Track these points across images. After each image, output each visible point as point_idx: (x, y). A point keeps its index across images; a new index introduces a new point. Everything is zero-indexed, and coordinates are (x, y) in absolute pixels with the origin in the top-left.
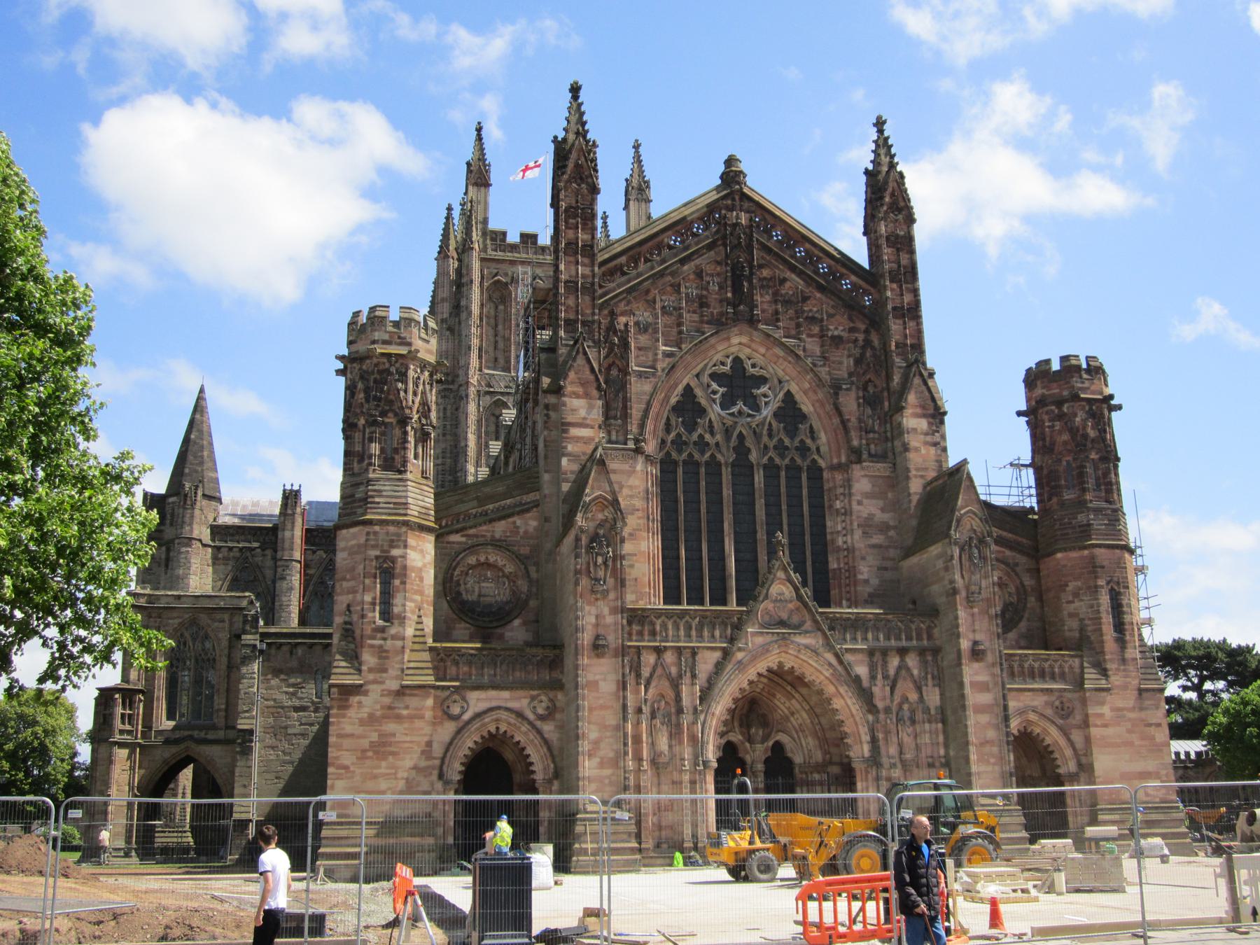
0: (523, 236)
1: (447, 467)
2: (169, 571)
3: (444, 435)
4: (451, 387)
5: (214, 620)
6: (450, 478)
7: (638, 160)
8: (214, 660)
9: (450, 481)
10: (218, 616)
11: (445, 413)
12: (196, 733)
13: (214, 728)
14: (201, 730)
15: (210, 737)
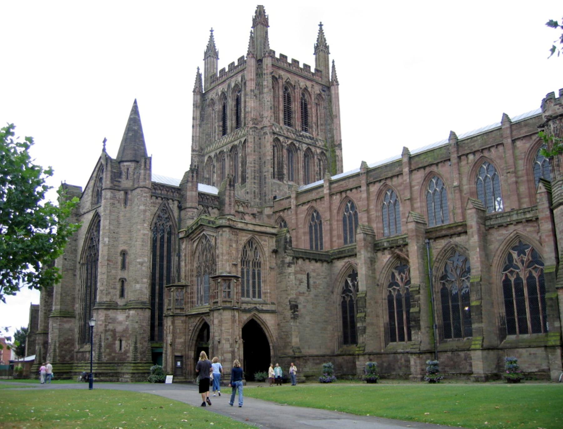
0: (281, 55)
1: (256, 169)
2: (128, 208)
3: (254, 151)
4: (257, 126)
5: (262, 240)
6: (258, 175)
7: (321, 32)
8: (260, 263)
9: (258, 177)
10: (263, 238)
11: (254, 140)
12: (257, 306)
13: (265, 303)
14: (260, 304)
15: (264, 308)
